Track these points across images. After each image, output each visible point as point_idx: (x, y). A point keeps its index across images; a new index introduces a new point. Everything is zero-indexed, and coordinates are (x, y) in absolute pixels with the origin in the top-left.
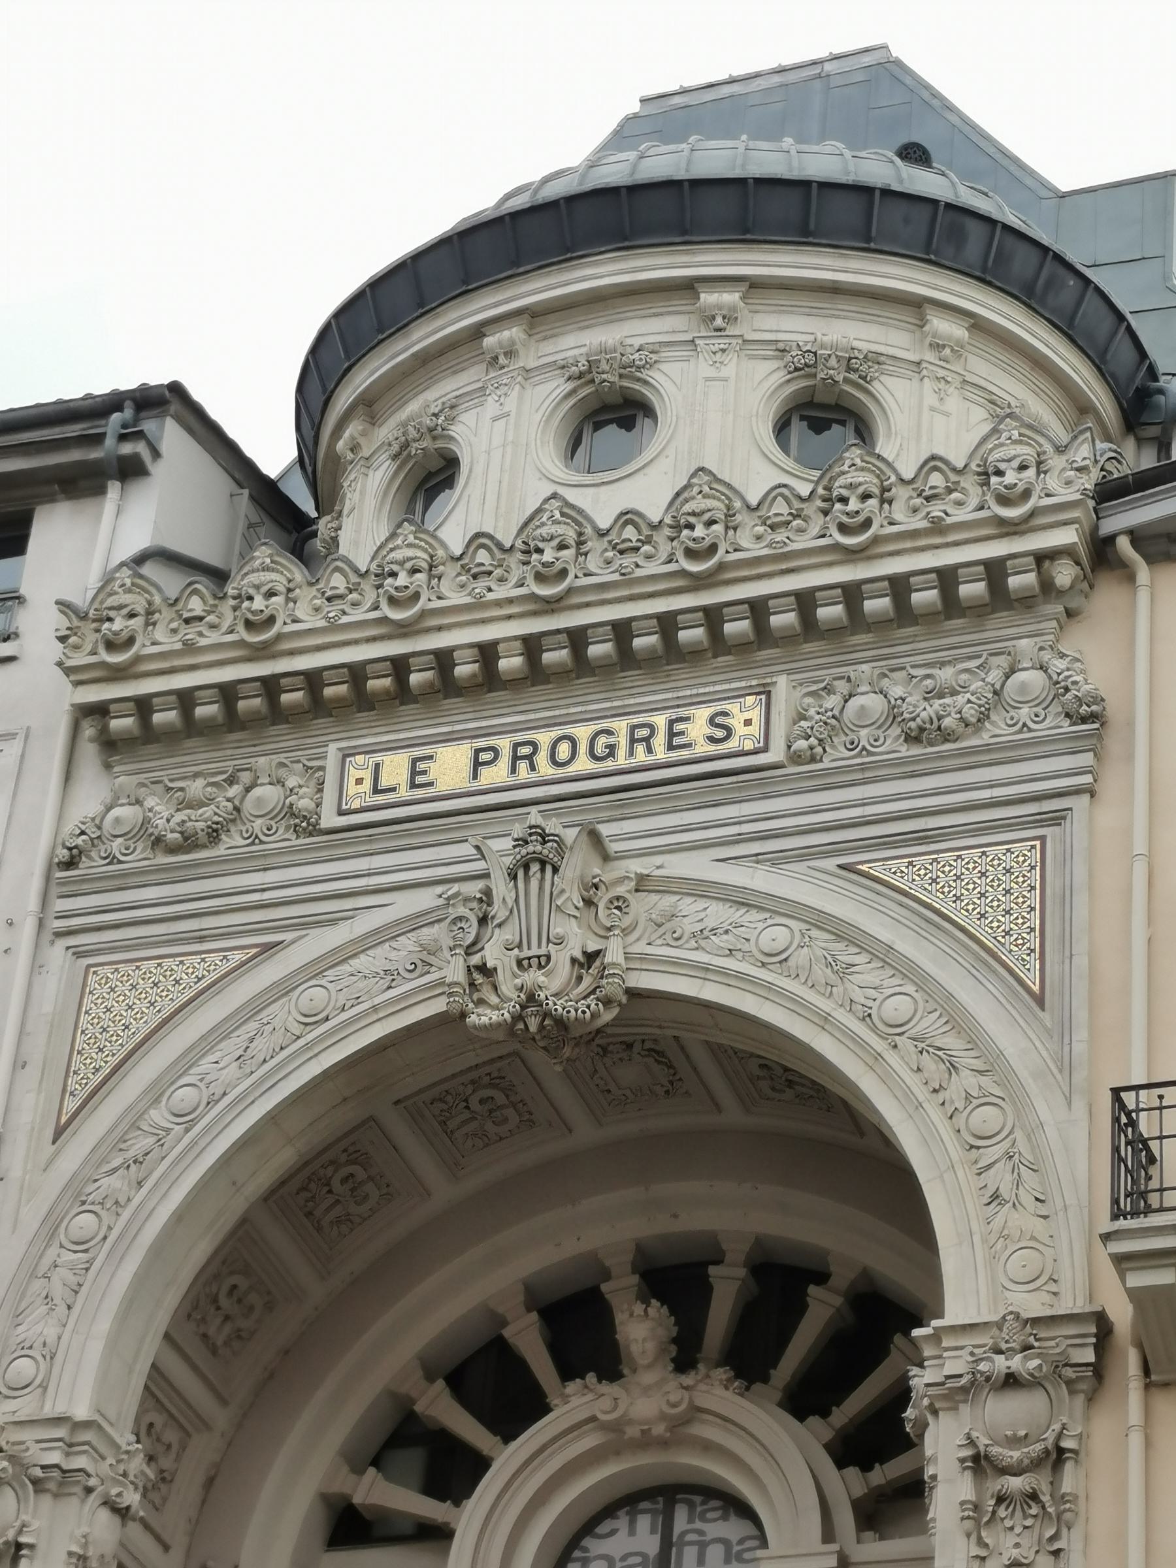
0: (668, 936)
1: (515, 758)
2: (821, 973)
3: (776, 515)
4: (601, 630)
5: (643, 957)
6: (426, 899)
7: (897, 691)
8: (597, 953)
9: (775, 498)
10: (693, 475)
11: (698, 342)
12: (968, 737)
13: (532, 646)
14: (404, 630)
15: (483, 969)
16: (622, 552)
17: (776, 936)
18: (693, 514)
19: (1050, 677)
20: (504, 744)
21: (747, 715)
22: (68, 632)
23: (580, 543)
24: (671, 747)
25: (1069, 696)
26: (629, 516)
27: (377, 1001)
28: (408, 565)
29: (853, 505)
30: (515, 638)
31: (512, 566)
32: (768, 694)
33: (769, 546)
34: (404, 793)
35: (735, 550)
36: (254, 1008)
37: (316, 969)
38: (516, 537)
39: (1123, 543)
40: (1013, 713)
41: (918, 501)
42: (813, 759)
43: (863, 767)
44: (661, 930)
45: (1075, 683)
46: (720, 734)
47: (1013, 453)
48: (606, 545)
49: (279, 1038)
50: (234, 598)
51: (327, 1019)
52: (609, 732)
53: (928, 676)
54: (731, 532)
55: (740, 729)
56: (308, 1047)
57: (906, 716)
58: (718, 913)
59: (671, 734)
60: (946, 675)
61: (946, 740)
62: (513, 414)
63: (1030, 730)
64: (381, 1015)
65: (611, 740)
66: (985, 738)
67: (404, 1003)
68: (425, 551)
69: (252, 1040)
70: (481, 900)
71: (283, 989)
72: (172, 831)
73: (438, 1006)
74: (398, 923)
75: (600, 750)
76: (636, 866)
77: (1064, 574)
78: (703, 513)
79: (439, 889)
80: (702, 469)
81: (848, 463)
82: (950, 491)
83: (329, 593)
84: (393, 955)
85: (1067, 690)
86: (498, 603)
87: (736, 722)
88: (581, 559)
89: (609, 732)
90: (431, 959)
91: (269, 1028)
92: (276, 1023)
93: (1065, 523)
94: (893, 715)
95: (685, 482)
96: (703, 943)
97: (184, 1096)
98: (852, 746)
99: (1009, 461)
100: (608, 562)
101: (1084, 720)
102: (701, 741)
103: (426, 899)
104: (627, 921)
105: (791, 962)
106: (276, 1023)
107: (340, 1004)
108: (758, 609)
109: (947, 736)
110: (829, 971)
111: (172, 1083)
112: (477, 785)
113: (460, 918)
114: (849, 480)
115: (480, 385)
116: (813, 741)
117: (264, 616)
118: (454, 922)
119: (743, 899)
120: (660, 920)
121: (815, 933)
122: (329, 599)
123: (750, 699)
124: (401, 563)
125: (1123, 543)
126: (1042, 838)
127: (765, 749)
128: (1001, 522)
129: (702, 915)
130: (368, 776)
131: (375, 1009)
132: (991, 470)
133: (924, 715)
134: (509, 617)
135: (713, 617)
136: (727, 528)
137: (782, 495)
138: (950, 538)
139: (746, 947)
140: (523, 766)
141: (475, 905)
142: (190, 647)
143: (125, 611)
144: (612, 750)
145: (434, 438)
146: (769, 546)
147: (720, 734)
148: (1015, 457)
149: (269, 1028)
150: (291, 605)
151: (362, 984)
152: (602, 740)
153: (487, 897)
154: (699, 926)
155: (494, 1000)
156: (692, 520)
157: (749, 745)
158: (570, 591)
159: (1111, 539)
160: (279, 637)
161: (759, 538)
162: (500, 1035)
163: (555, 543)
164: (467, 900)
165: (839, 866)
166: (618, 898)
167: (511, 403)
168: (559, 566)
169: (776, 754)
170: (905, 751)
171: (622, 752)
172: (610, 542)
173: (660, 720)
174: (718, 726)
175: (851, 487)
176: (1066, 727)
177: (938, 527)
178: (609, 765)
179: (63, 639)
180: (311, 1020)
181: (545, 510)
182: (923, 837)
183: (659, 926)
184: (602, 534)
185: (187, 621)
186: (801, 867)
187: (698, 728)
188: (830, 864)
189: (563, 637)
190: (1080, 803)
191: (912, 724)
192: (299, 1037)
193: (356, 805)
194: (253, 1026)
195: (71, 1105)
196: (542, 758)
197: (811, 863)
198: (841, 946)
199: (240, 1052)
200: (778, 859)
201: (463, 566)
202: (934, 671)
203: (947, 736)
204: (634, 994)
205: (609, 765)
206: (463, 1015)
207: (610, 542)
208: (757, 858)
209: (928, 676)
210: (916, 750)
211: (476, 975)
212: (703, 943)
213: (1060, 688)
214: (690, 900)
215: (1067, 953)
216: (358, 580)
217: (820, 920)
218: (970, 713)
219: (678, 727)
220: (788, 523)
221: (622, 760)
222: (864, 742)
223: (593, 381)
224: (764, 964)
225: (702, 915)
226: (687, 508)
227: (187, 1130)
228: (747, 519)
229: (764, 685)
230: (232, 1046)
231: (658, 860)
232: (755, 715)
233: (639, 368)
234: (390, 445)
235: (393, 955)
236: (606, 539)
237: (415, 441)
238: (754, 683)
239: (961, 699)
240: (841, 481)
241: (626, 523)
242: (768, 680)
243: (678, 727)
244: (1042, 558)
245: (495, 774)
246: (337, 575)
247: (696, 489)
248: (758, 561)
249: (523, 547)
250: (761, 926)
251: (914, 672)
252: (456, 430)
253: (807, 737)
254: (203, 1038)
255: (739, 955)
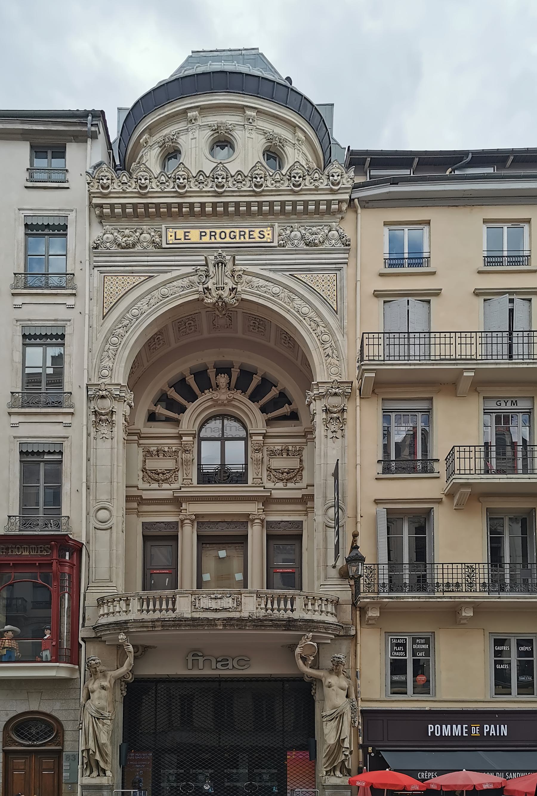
0: (250, 286)
1: (211, 235)
2: (287, 300)
3: (277, 178)
4: (232, 203)
5: (245, 291)
6: (190, 270)
7: (304, 232)
8: (235, 288)
9: (276, 174)
10: (257, 163)
11: (245, 125)
12: (320, 246)
13: (214, 205)
14: (181, 196)
15: (207, 288)
16: (238, 182)
17: (276, 289)
18: (257, 174)
19: (339, 234)
20: (208, 231)
21: (268, 232)
22: (90, 182)
23: (227, 178)
24: (250, 238)
25: (344, 239)
26: (239, 172)
27: (181, 293)
28: (183, 177)
29: (297, 179)
30: (210, 202)
31: (209, 182)
32: (273, 227)
33: (275, 187)
34: (183, 241)
35: (267, 187)
36: (149, 292)
37: (165, 284)
38: (210, 174)
39: (356, 200)
40: (330, 241)
41: (312, 181)
42: (283, 247)
43: (296, 250)
44: (248, 285)
45: (346, 236)
46: (262, 236)
47: (337, 171)
48: (233, 180)
49: (157, 300)
50: (136, 179)
51: (168, 297)
52: (234, 232)
53: (310, 229)
54: (265, 181)
55: (266, 236)
56: (164, 303)
57: (306, 238)
58: (262, 282)
59: (250, 235)
60: (314, 229)
61: (315, 246)
62: (197, 138)
63: (334, 246)
64: (182, 297)
65: (235, 234)
66: (324, 247)
67: (186, 295)
68: (187, 173)
69: (150, 300)
70: (206, 271)
71: (156, 288)
72: (123, 243)
73: (196, 297)
74: (183, 275)
75: (232, 236)
76: (243, 268)
77: (344, 206)
78: (260, 174)
79: (193, 267)
80: (259, 162)
81: (296, 167)
82: (320, 179)
83: (161, 182)
84: (183, 283)
85: (343, 237)
86: (206, 192)
87: (265, 234)
88: (227, 182)
89: (234, 232)
90: (192, 285)
91: (154, 297)
92: (155, 296)
93: (346, 193)
94: (303, 237)
95: (254, 165)
96: (259, 289)
97: (135, 312)
98: (292, 244)
99: (336, 173)
100: (234, 185)
101: (346, 246)
102: (257, 237)
103: (190, 270)
104: (241, 281)
105: (280, 296)
106: (155, 296)
107: (171, 293)
108: (271, 204)
109: (316, 245)
110: (289, 299)
111: (131, 308)
112: (201, 241)
113: (201, 275)
114: (297, 172)
115: (186, 128)
116: (284, 241)
117: (144, 185)
118: (199, 276)
119: (267, 279)
120: (248, 282)
121: (285, 290)
122: (161, 183)
123: (269, 228)
124: (181, 176)
125: (356, 200)
126: (336, 274)
127: (273, 242)
128: (331, 190)
129: (258, 282)
130: (173, 234)
131: (180, 295)
132: (331, 175)
133: (311, 239)
134: (208, 196)
135: (260, 204)
136: (264, 180)
137: (278, 173)
138: (319, 192)
139: (269, 291)
140: (213, 238)
141: (204, 272)
142: (124, 192)
143: (106, 178)
144: (235, 236)
145: (172, 142)
146: (275, 187)
147: (262, 236)
148: (337, 172)
149: (154, 297)
150: (151, 183)
151: (176, 289)
152: (232, 234)
153: (207, 271)
154: (257, 285)
155: (210, 297)
156: (257, 176)
157: (269, 241)
158: (225, 191)
159: (354, 199)
160: (148, 192)
161: (272, 184)
162: (211, 306)
163: (222, 177)
164: (202, 271)
165: (290, 274)
166: (239, 275)
167: (196, 135)
168: (222, 183)
169: (275, 244)
170: (305, 247)
171: (238, 237)
172: (234, 179)
173: (247, 231)
174: (261, 234)
175: (297, 173)
176: (342, 247)
177: (317, 189)
178: (234, 240)
179: (89, 183)
180: (164, 296)
181: (218, 167)
182: (309, 270)
183: (248, 283)
184: (232, 177)
185: (123, 183)
186: (280, 273)
187: (256, 234)
188: (287, 273)
189: (222, 204)
190: (345, 266)
191: (308, 241)
192: (161, 300)
193: (171, 242)
194: (149, 296)
195: (106, 311)
196: (217, 236)
197: (283, 273)
198: (291, 294)
199: (147, 302)
200: (275, 271)
201: (196, 180)
202: (311, 228)
203: (316, 245)
204: (242, 300)
205: (234, 240)
206: (203, 300)
207: (234, 179)
208: (270, 270)
209: (310, 229)
210: (308, 248)
211: (205, 290)
212: (259, 289)
213: (341, 237)
214: (255, 278)
215: (342, 302)
216: (168, 179)
217: (286, 287)
218: (321, 239)
219: (251, 233)
220: (280, 181)
221: (237, 240)
222: (296, 244)
223: (218, 132)
224: (273, 296)
225: (258, 282)
226: (256, 172)
227: (137, 320)
228: (269, 179)
229: (272, 225)
230: (145, 301)
231: (247, 267)
232: (270, 232)
233: (230, 131)
234: (159, 143)
235: (183, 283)
236: (233, 178)
237: (168, 142)
238: (270, 224)
239: (320, 236)
240: (295, 171)
241: (239, 174)
242: (273, 224)
243: (251, 233)
244: (340, 201)
245: (206, 239)
246: (163, 176)
247: (257, 168)
248: (272, 191)
249: (212, 177)
250: (272, 287)
251: (307, 227)
252: (179, 141)
253: (283, 241)
254: (138, 298)
255: (267, 293)
